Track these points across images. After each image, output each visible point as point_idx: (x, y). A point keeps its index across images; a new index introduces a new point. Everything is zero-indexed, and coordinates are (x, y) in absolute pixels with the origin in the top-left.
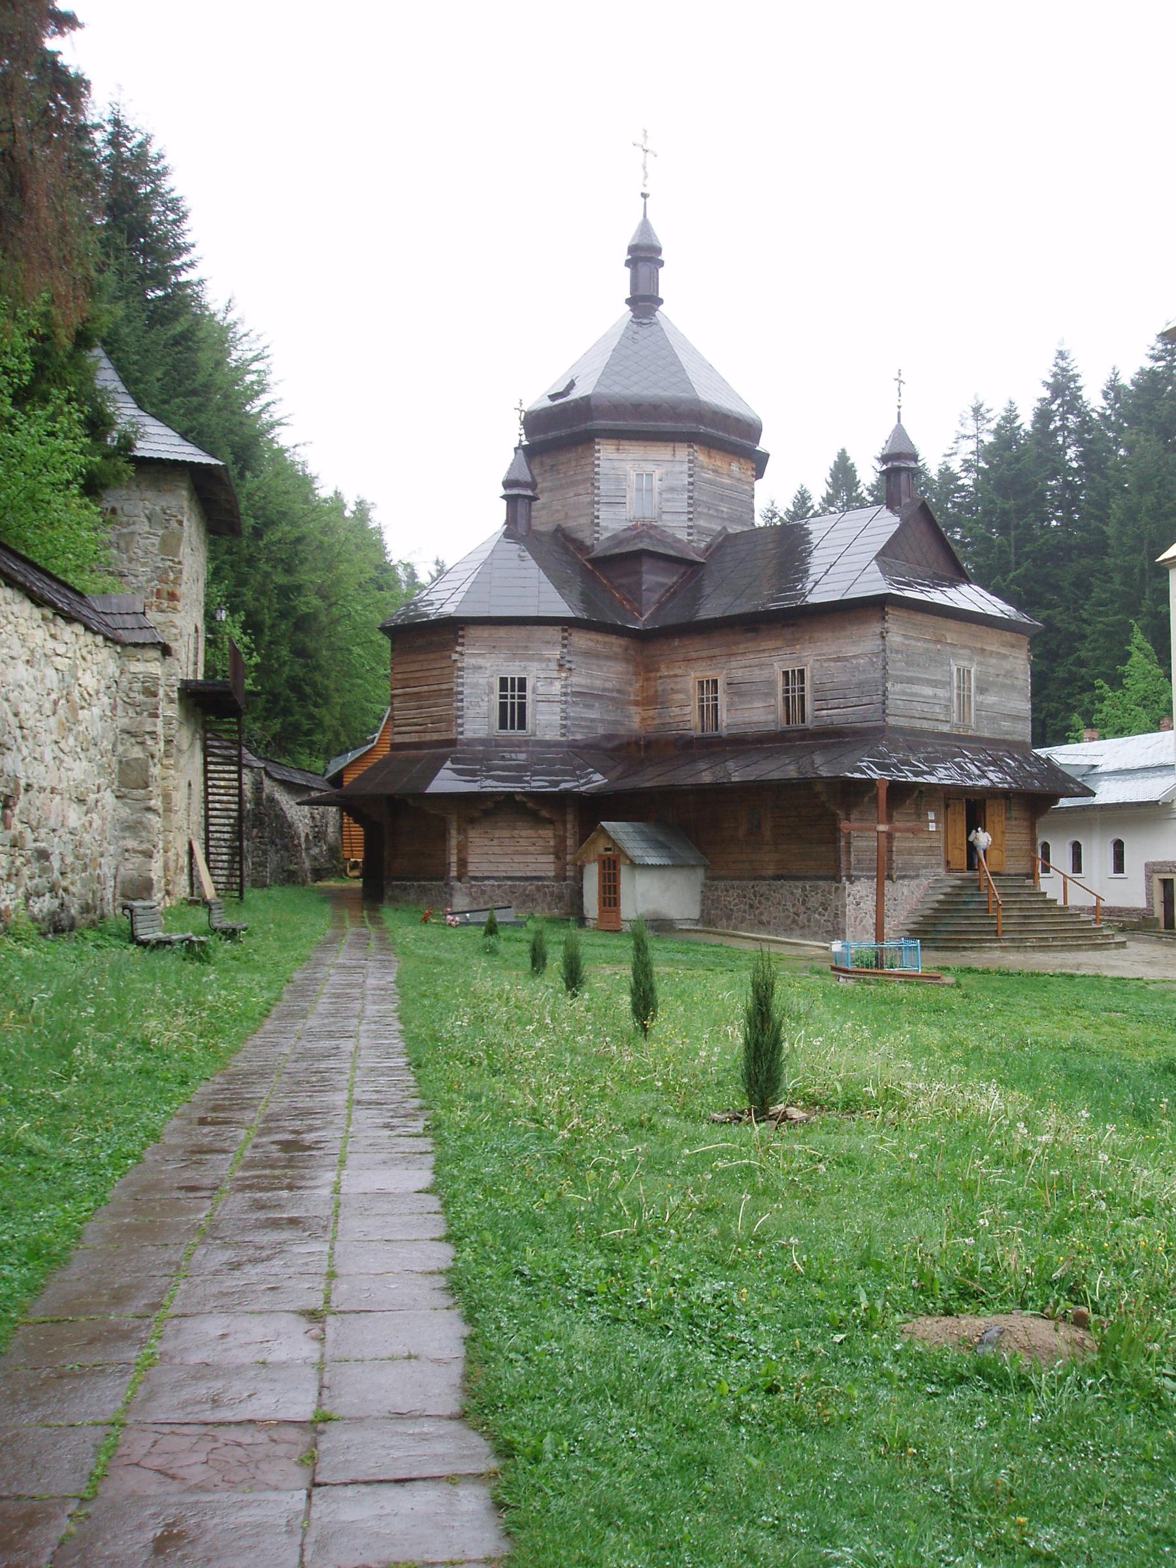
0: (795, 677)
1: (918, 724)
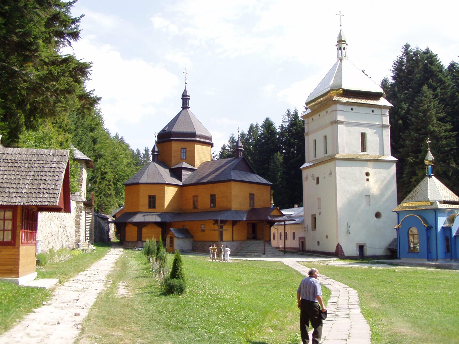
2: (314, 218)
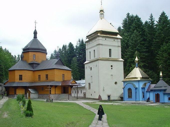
2: (90, 84)
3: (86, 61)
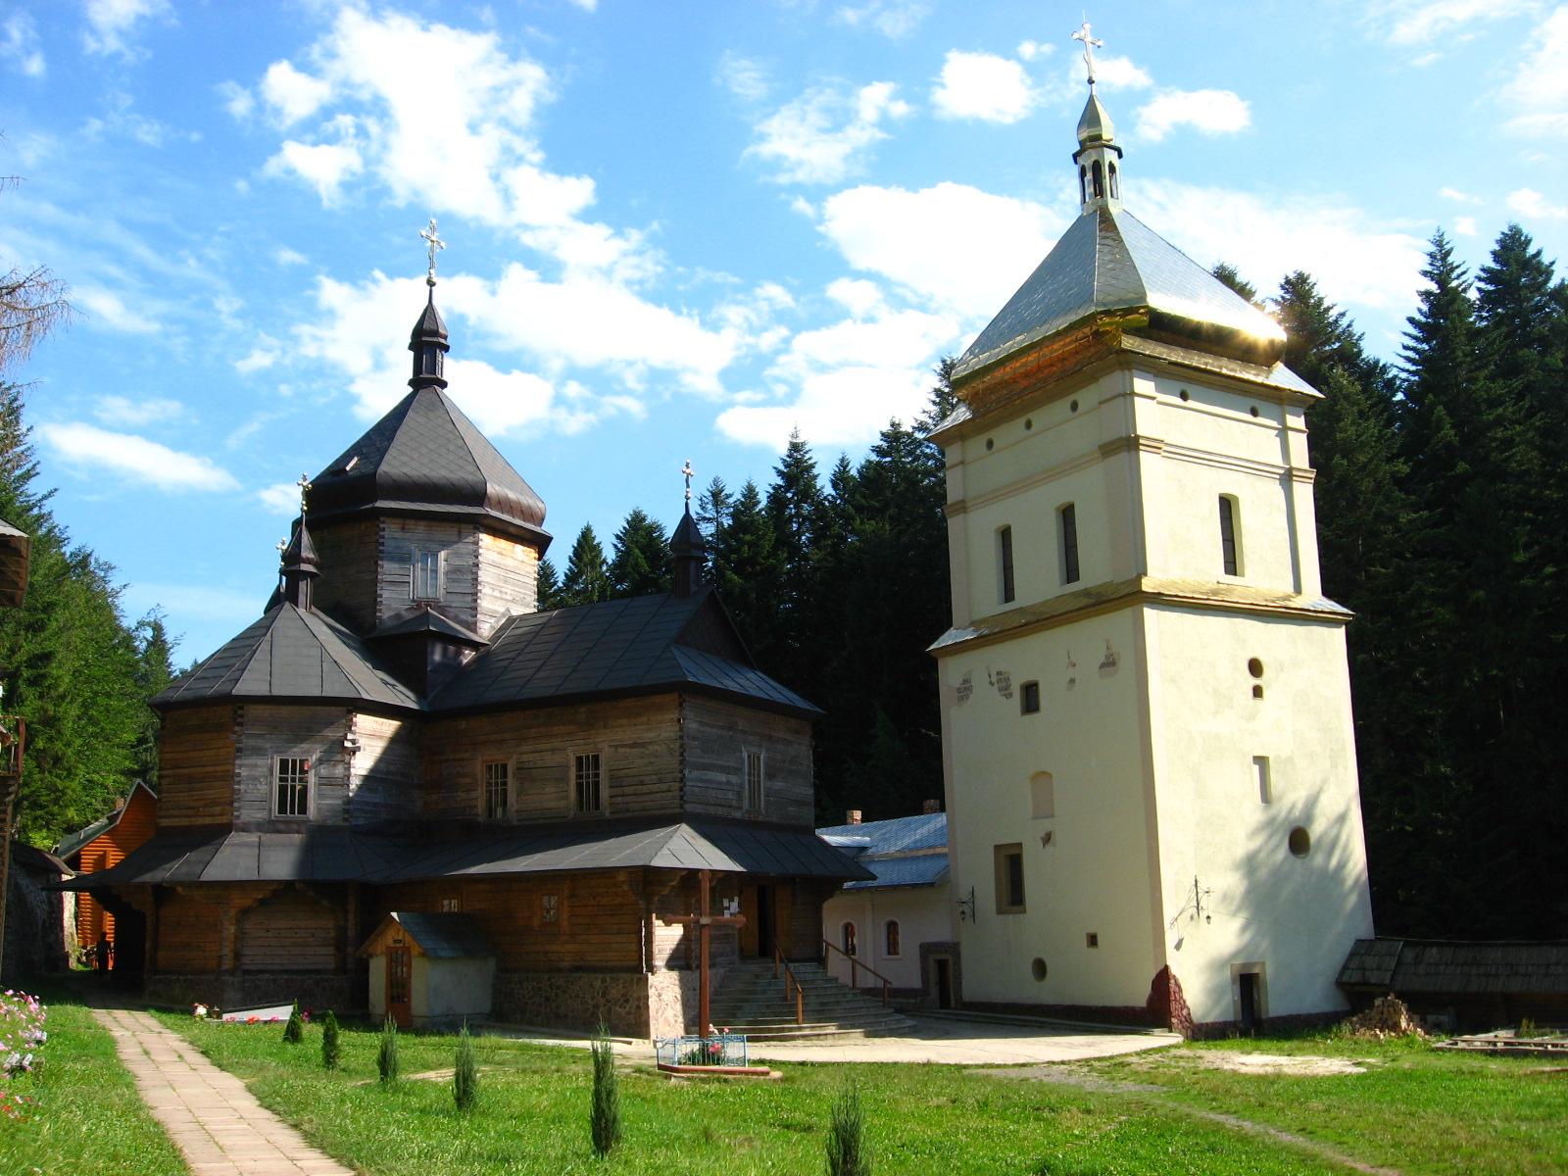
0: (589, 764)
1: (712, 810)
3: (949, 625)
